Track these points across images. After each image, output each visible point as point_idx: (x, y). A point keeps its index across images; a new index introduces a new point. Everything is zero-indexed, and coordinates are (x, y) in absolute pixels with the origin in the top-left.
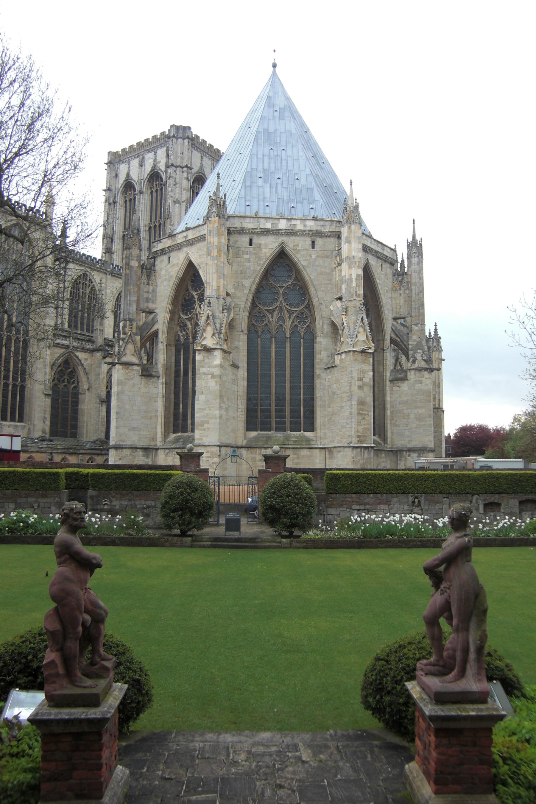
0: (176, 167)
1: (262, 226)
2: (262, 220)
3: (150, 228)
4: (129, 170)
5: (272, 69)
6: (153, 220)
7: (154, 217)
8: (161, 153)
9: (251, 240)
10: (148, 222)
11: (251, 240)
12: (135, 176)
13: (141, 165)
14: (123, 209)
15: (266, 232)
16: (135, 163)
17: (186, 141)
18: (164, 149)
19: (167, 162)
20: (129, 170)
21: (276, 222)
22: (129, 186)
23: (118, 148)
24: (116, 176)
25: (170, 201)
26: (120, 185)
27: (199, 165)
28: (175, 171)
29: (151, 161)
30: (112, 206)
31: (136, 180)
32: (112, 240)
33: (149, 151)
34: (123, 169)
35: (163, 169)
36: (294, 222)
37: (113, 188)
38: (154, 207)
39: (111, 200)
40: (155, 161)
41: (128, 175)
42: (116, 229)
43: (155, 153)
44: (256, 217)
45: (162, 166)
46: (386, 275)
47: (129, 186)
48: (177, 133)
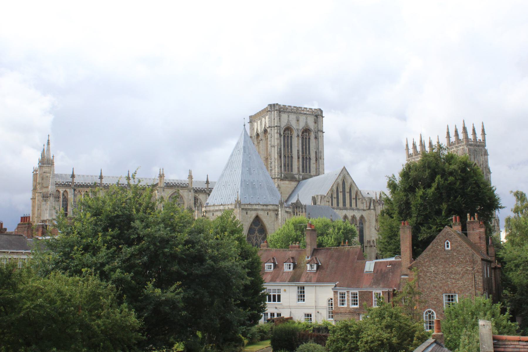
0: (272, 127)
1: (215, 209)
2: (215, 207)
4: (257, 127)
5: (244, 127)
9: (213, 214)
11: (213, 214)
12: (259, 131)
15: (217, 211)
16: (259, 122)
17: (276, 112)
21: (219, 207)
22: (258, 135)
27: (286, 121)
28: (271, 130)
36: (225, 206)
37: (253, 136)
41: (257, 130)
43: (265, 118)
44: (214, 205)
46: (271, 216)
48: (271, 108)
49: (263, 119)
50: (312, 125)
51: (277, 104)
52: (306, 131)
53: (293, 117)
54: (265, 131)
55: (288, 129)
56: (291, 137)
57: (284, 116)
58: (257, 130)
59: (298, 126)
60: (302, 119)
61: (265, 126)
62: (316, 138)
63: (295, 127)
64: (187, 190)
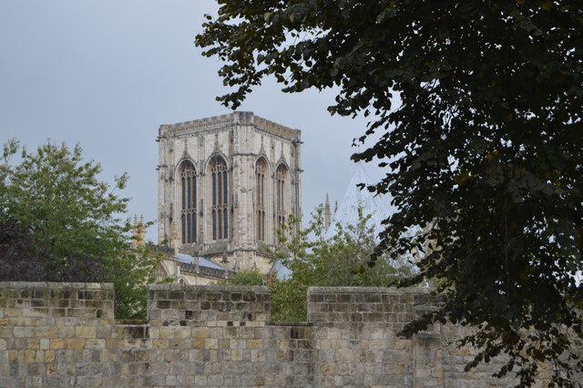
0: (241, 155)
3: (214, 211)
4: (186, 148)
6: (217, 204)
7: (217, 204)
8: (223, 136)
10: (211, 205)
12: (194, 155)
13: (201, 144)
14: (181, 187)
18: (226, 134)
19: (231, 149)
20: (186, 148)
22: (187, 164)
23: (172, 121)
24: (171, 151)
25: (237, 191)
26: (176, 163)
29: (212, 143)
30: (168, 183)
31: (196, 160)
32: (171, 219)
33: (209, 132)
34: (179, 145)
35: (227, 153)
37: (168, 164)
38: (217, 191)
39: (168, 176)
40: (216, 143)
41: (185, 153)
42: (174, 208)
45: (225, 151)
47: (187, 164)
49: (210, 138)
50: (289, 160)
51: (252, 113)
52: (282, 167)
53: (267, 140)
54: (217, 159)
55: (262, 161)
56: (263, 176)
57: (258, 136)
58: (185, 153)
59: (274, 158)
60: (278, 143)
61: (216, 149)
62: (292, 183)
63: (269, 158)
64: (172, 262)
